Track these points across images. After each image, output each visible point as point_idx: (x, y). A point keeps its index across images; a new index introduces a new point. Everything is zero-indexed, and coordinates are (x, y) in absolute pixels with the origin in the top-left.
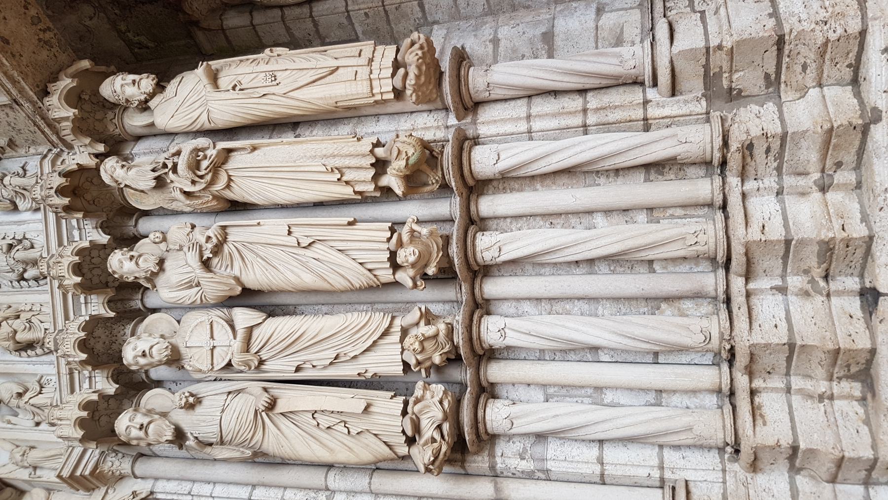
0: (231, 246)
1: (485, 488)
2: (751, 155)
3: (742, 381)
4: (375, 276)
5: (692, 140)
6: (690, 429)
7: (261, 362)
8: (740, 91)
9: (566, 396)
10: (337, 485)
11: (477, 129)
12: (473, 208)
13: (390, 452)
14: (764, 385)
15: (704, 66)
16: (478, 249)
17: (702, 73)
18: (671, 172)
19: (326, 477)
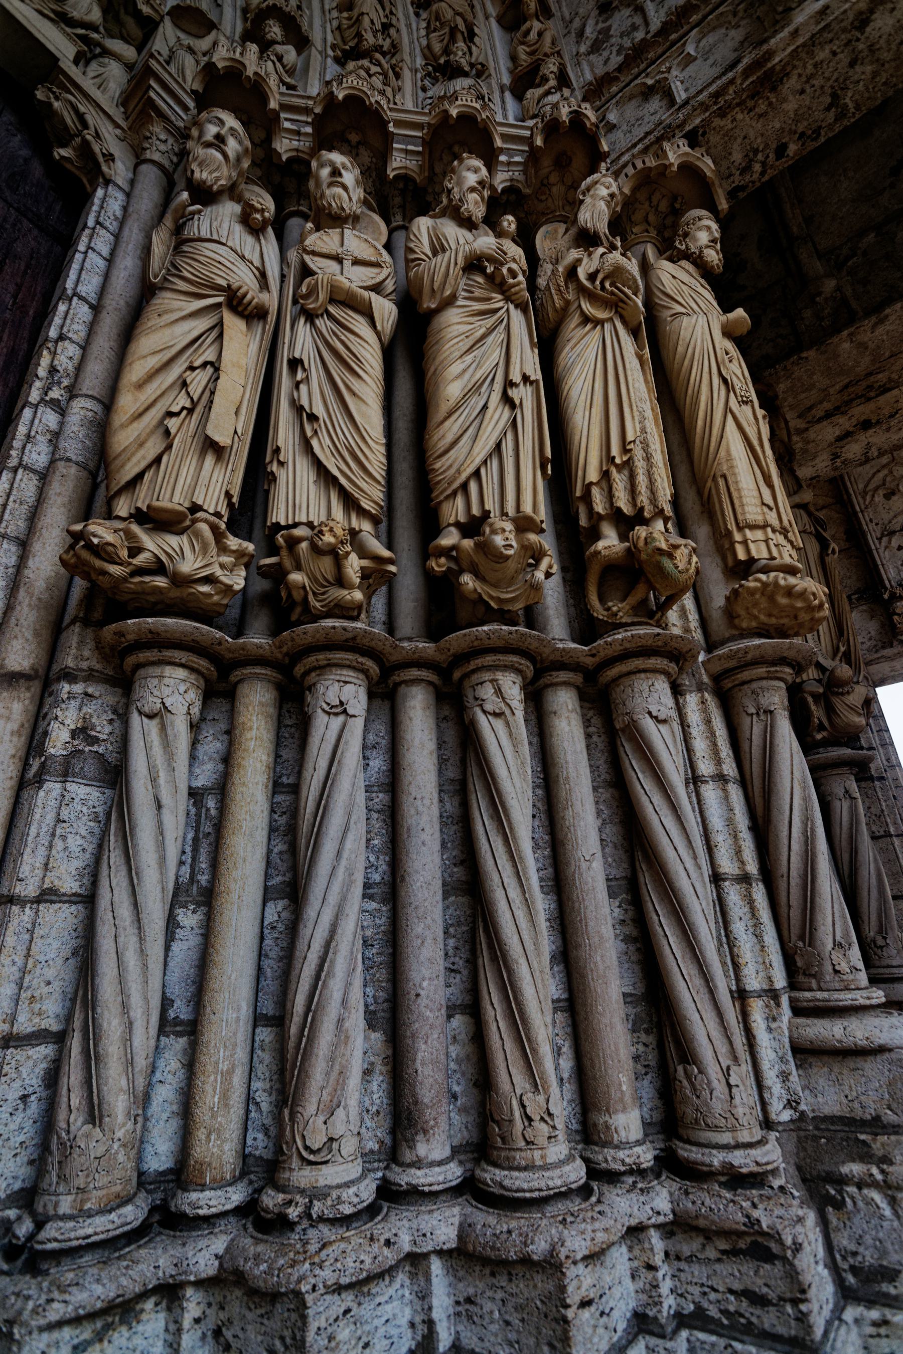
0: (501, 304)
1: (20, 654)
2: (734, 1253)
3: (204, 1255)
4: (454, 493)
5: (737, 1101)
6: (95, 1114)
7: (310, 317)
8: (839, 1205)
9: (197, 831)
10: (74, 411)
11: (691, 692)
12: (563, 676)
13: (123, 482)
14: (187, 1322)
15: (877, 1119)
16: (499, 675)
17: (859, 1113)
18: (641, 1048)
19: (92, 397)
